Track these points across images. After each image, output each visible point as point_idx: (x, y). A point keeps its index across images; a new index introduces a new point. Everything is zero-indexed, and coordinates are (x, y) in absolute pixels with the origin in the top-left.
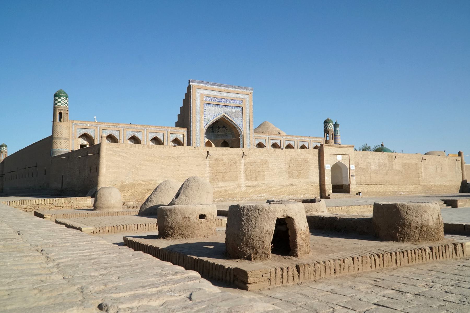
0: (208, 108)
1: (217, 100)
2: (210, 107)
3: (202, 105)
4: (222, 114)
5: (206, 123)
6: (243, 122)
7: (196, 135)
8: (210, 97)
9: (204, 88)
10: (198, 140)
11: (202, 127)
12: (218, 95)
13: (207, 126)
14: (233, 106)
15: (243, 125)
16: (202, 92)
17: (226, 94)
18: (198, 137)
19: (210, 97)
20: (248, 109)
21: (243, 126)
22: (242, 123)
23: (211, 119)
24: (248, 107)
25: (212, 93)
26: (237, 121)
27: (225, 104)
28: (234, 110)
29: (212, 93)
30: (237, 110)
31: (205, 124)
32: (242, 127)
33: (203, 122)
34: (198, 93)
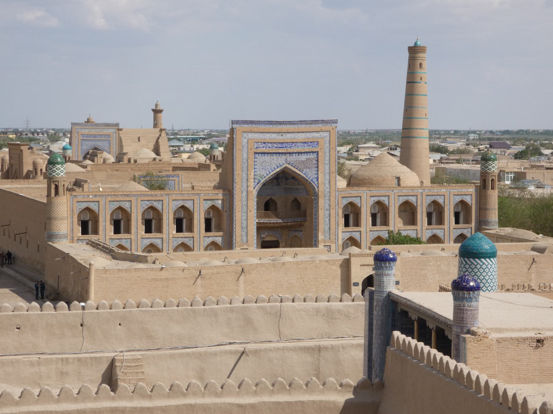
0: (260, 158)
1: (275, 145)
3: (252, 156)
4: (284, 166)
5: (257, 181)
6: (318, 174)
7: (241, 201)
8: (264, 143)
9: (255, 130)
10: (245, 207)
11: (251, 189)
13: (259, 186)
14: (301, 153)
15: (317, 178)
16: (251, 136)
17: (289, 135)
18: (245, 203)
19: (264, 143)
20: (328, 154)
21: (318, 180)
22: (316, 176)
23: (265, 175)
24: (327, 150)
25: (267, 137)
26: (308, 174)
27: (290, 150)
28: (303, 157)
29: (267, 137)
30: (308, 157)
31: (256, 183)
33: (252, 180)
34: (245, 138)
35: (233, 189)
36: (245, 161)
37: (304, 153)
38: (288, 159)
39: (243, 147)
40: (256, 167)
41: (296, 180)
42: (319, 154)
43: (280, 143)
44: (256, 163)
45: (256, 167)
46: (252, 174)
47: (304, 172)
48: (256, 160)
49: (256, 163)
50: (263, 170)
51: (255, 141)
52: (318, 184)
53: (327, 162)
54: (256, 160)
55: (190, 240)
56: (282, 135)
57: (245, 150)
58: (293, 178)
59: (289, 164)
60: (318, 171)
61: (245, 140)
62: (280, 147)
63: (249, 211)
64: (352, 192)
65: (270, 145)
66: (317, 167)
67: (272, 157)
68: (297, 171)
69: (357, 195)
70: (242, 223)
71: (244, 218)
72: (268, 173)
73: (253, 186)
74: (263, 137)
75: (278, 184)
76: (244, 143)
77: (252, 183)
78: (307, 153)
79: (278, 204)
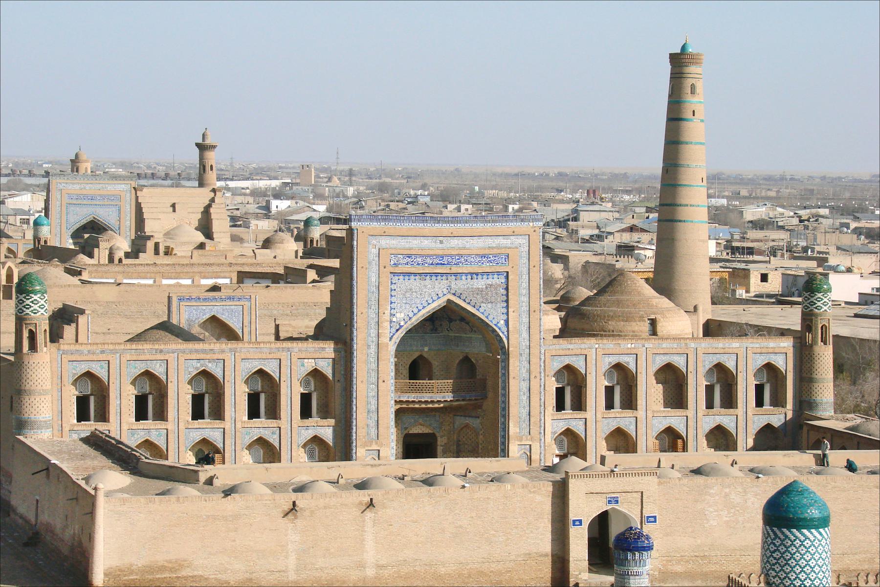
0: (402, 283)
1: (429, 261)
2: (407, 283)
3: (386, 278)
6: (507, 314)
9: (392, 232)
10: (374, 374)
11: (384, 340)
12: (433, 245)
13: (401, 334)
15: (507, 322)
16: (384, 242)
17: (455, 242)
20: (525, 277)
23: (411, 315)
24: (525, 270)
25: (415, 243)
26: (490, 313)
27: (455, 269)
28: (480, 283)
29: (415, 243)
31: (394, 330)
32: (504, 329)
35: (352, 340)
36: (374, 289)
37: (483, 273)
38: (453, 286)
39: (370, 263)
40: (393, 300)
41: (468, 323)
42: (510, 278)
43: (437, 256)
44: (393, 293)
45: (393, 300)
46: (388, 312)
47: (481, 310)
48: (393, 287)
49: (393, 293)
50: (408, 306)
51: (393, 252)
52: (508, 331)
53: (525, 292)
54: (393, 287)
55: (273, 433)
56: (441, 242)
57: (375, 268)
58: (462, 319)
59: (454, 294)
60: (507, 307)
61: (375, 251)
62: (437, 264)
63: (381, 381)
64: (571, 346)
65: (419, 260)
66: (507, 301)
67: (423, 282)
68: (469, 308)
69: (578, 352)
70: (368, 403)
71: (374, 393)
72: (416, 311)
73: (389, 336)
74: (407, 246)
75: (435, 330)
76: (371, 257)
77: (386, 331)
78: (488, 273)
79: (434, 367)
